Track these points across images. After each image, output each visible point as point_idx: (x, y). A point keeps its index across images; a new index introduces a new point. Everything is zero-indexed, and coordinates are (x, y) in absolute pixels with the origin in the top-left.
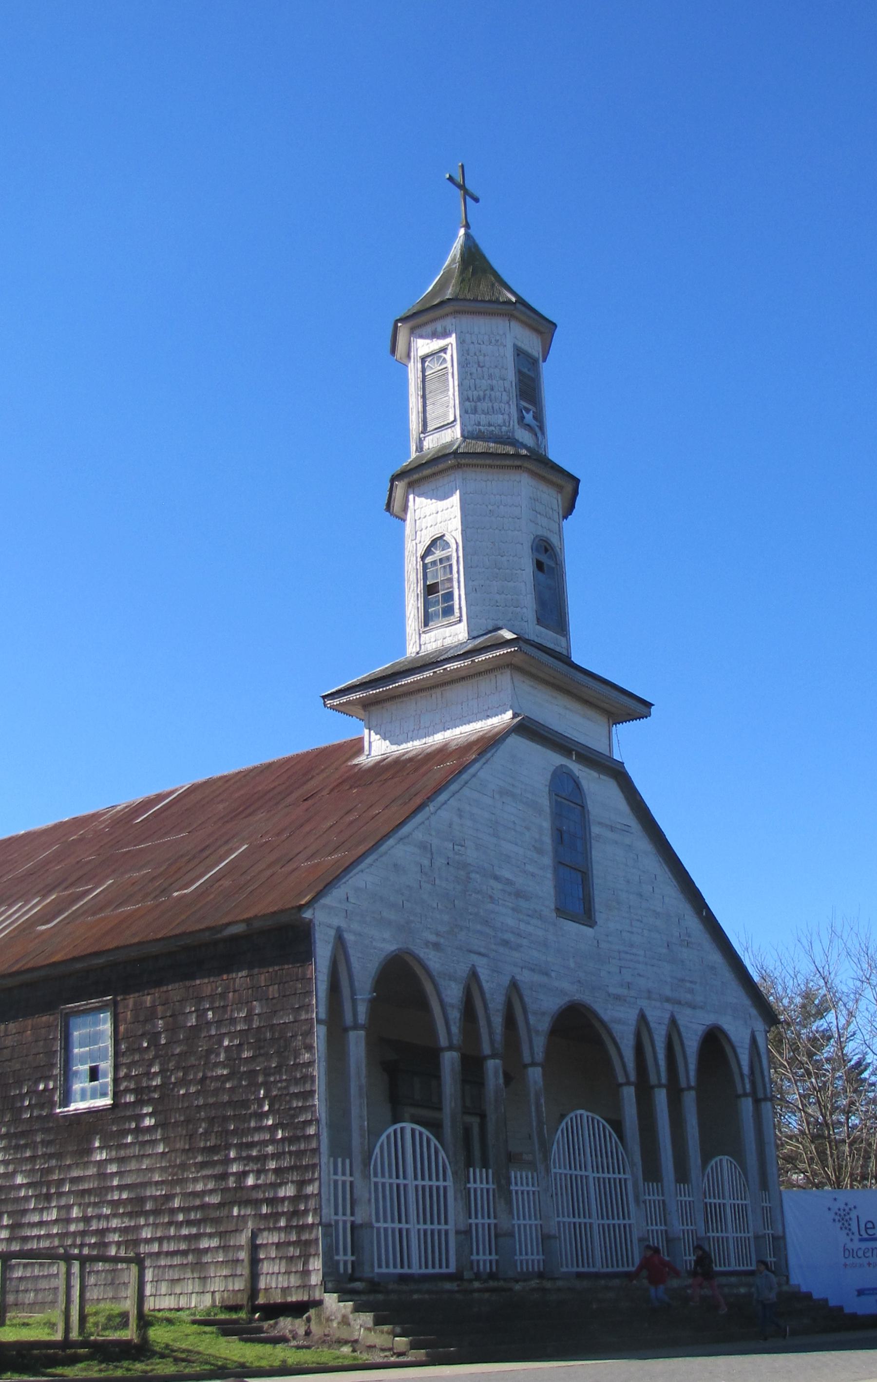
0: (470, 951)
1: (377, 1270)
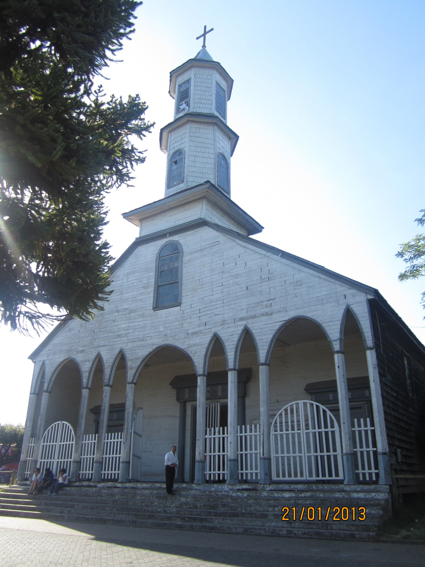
0: (99, 347)
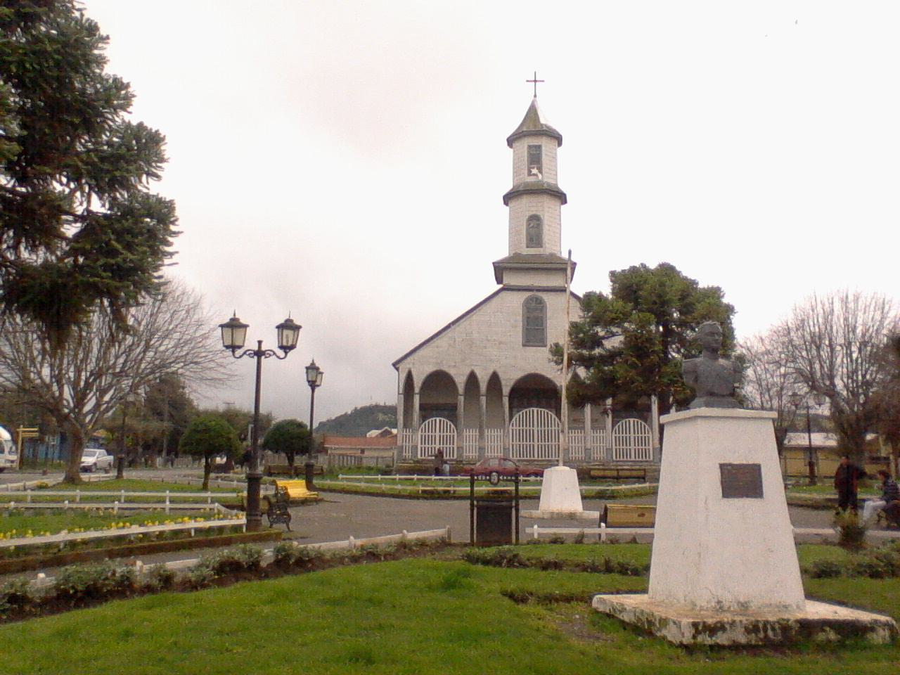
1: (419, 457)
